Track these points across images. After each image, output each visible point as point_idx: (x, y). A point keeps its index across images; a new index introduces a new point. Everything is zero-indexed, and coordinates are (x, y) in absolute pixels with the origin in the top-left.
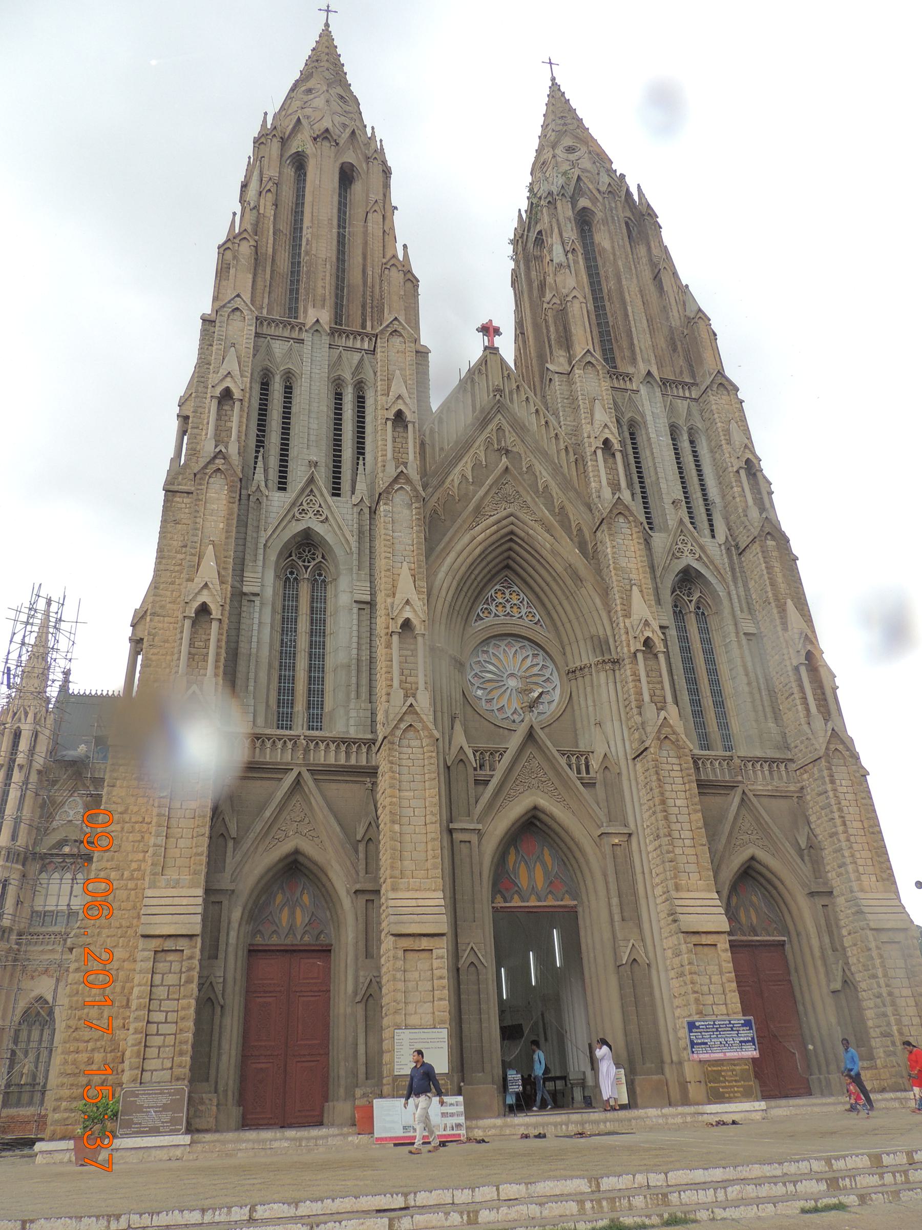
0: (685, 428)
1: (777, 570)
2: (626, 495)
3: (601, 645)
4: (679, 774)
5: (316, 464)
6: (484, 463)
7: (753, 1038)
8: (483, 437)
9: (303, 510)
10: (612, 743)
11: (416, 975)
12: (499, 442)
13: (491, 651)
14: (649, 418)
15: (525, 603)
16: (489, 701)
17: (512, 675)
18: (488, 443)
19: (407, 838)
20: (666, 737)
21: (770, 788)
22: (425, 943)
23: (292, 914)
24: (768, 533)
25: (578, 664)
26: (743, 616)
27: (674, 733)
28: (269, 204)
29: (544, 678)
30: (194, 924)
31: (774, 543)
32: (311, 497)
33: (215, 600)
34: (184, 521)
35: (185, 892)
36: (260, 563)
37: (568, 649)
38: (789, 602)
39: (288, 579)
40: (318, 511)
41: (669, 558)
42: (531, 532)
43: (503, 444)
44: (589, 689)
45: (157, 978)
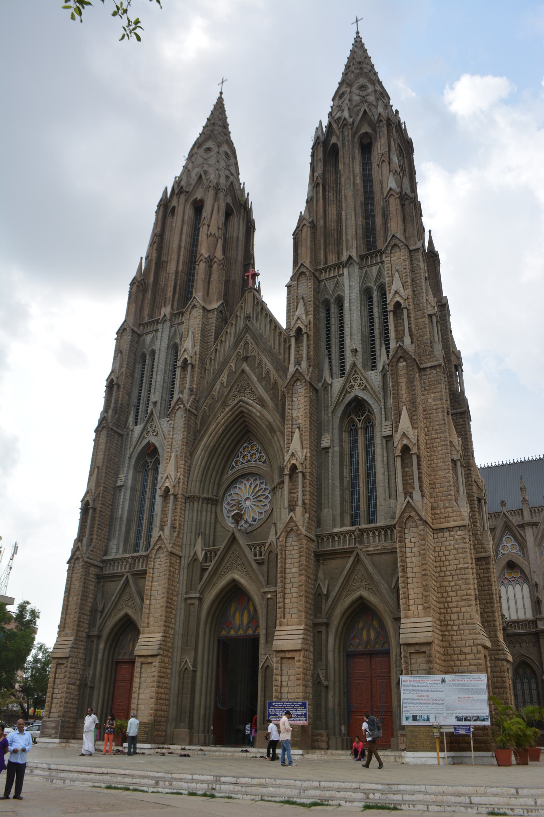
0: (375, 287)
1: (403, 384)
5: (155, 403)
7: (305, 714)
8: (236, 353)
11: (146, 675)
13: (238, 486)
14: (347, 292)
18: (239, 354)
19: (153, 607)
20: (292, 529)
21: (379, 548)
22: (150, 660)
24: (401, 357)
26: (388, 423)
27: (297, 526)
28: (154, 250)
31: (404, 363)
36: (126, 468)
41: (343, 395)
42: (250, 408)
45: (57, 675)
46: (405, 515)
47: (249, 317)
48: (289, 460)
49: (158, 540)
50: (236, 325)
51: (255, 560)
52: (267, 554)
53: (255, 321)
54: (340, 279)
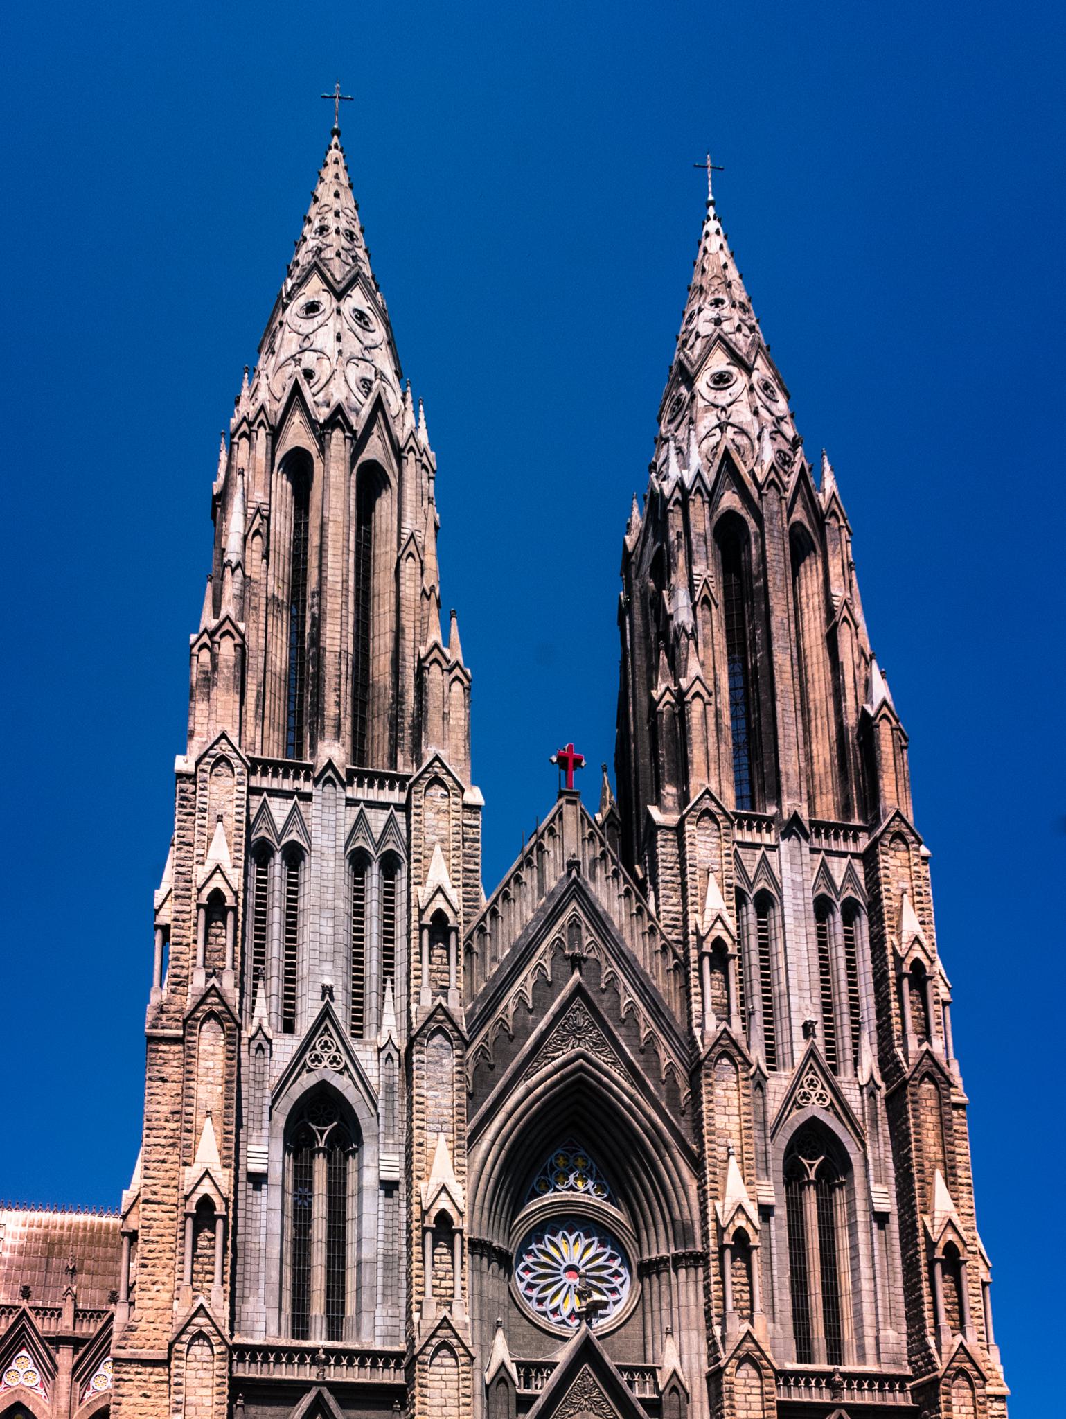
1: (930, 1126)
2: (736, 1028)
3: (682, 1233)
4: (759, 1398)
6: (549, 979)
9: (316, 1056)
10: (685, 1357)
12: (571, 946)
15: (594, 1172)
16: (540, 1301)
17: (571, 1269)
18: (558, 946)
25: (654, 1255)
29: (611, 1271)
31: (932, 1087)
32: (326, 1038)
34: (175, 1078)
36: (265, 1132)
37: (644, 1233)
38: (939, 1175)
39: (297, 1141)
40: (335, 1057)
42: (606, 1079)
43: (577, 951)
44: (664, 1288)
46: (955, 1365)
47: (578, 863)
48: (732, 1219)
49: (439, 1327)
50: (541, 871)
51: (641, 1400)
52: (667, 1391)
53: (588, 879)
54: (772, 857)
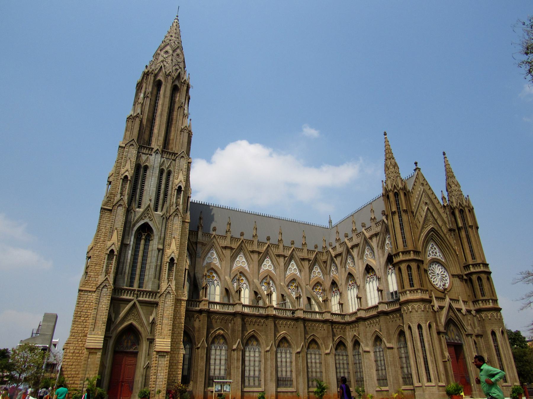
22: (165, 354)
23: (127, 342)
30: (101, 346)
33: (116, 249)
35: (100, 337)
